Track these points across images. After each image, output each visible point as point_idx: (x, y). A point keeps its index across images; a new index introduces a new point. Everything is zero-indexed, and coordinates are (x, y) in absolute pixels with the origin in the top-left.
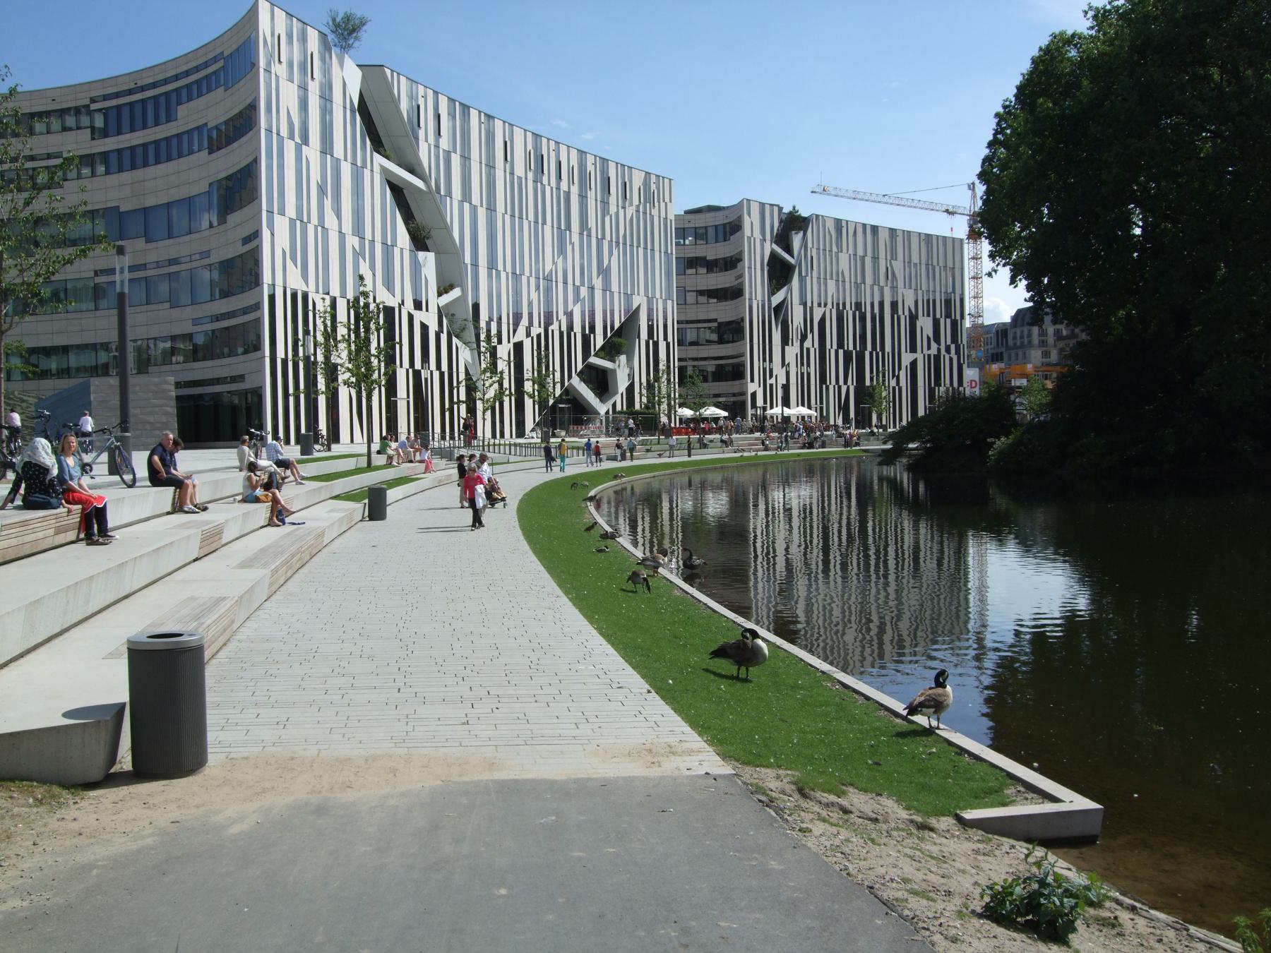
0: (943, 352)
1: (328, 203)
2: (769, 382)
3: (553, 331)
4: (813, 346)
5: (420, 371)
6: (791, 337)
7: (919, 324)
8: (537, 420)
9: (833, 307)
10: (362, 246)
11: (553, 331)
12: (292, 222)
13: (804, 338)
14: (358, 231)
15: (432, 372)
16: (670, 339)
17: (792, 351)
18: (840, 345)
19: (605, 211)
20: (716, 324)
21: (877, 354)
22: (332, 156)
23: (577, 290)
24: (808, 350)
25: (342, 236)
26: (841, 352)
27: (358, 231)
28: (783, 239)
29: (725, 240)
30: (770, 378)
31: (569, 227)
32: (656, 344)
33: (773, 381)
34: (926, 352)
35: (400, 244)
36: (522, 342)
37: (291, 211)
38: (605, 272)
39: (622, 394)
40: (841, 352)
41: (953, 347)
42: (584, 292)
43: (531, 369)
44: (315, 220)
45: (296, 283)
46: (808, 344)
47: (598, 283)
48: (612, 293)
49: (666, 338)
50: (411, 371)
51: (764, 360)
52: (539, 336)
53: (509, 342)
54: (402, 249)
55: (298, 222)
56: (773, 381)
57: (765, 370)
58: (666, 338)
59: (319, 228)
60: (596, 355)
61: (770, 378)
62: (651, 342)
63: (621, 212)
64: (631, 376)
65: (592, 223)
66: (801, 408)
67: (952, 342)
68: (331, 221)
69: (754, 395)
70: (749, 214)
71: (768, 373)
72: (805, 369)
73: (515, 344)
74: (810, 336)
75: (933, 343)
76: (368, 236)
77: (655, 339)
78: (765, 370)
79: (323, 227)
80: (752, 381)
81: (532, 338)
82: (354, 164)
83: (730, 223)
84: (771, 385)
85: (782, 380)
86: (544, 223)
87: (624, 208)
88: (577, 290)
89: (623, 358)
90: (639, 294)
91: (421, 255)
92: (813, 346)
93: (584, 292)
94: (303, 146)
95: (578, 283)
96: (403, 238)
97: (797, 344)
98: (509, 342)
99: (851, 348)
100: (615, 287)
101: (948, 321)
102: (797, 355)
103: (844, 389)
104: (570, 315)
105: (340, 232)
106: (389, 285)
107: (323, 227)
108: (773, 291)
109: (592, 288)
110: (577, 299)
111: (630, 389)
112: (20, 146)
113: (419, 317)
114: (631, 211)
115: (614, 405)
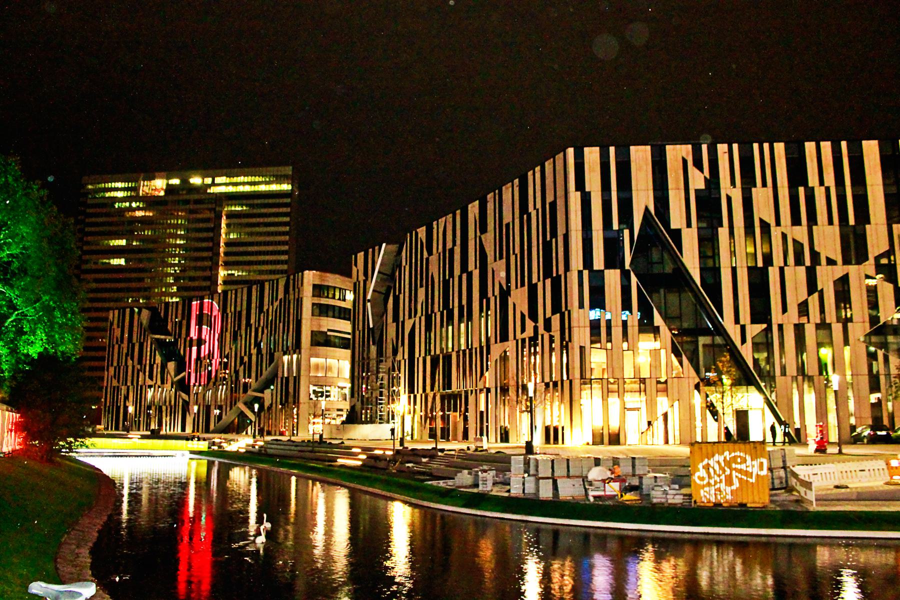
1: (129, 358)
9: (422, 315)
12: (115, 368)
13: (395, 352)
14: (140, 362)
23: (242, 358)
25: (133, 367)
27: (140, 362)
31: (240, 328)
34: (519, 336)
37: (115, 364)
41: (556, 320)
42: (246, 359)
44: (123, 364)
46: (399, 357)
47: (254, 351)
48: (262, 355)
63: (271, 307)
65: (252, 321)
68: (130, 362)
70: (356, 265)
74: (400, 349)
75: (528, 321)
76: (144, 362)
86: (226, 331)
87: (272, 304)
88: (242, 358)
90: (278, 351)
93: (246, 359)
95: (243, 354)
99: (438, 352)
101: (548, 282)
103: (431, 395)
106: (151, 378)
109: (250, 355)
110: (242, 362)
114: (276, 304)
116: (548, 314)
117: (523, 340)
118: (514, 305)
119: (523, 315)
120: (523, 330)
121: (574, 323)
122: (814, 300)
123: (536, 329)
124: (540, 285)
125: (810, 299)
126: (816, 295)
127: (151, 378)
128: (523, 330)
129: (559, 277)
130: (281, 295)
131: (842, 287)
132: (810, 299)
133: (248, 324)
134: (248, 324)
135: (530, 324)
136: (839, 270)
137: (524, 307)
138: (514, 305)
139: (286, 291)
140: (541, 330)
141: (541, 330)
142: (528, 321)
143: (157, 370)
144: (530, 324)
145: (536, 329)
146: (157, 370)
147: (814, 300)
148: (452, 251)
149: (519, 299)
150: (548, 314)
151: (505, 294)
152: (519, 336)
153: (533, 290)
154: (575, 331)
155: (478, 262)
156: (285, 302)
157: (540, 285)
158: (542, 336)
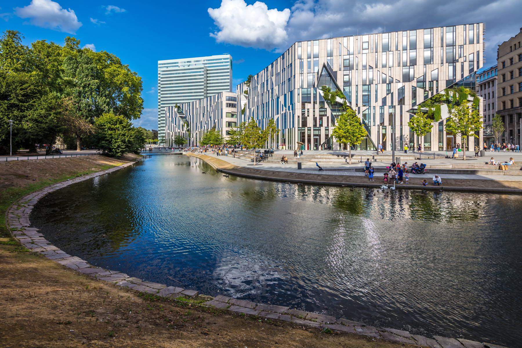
7: (280, 100)
19: (211, 106)
34: (282, 113)
38: (210, 117)
42: (207, 122)
45: (168, 131)
47: (209, 120)
65: (208, 110)
72: (491, 101)
75: (284, 107)
93: (207, 122)
100: (212, 120)
101: (289, 93)
104: (204, 127)
106: (179, 129)
112: (137, 124)
113: (183, 132)
114: (215, 103)
116: (289, 105)
119: (283, 105)
120: (283, 110)
121: (296, 108)
122: (389, 98)
123: (286, 109)
124: (287, 94)
125: (387, 96)
126: (390, 95)
127: (179, 129)
128: (283, 110)
129: (292, 91)
130: (216, 100)
131: (402, 91)
132: (387, 96)
133: (207, 111)
134: (207, 111)
135: (284, 108)
136: (400, 85)
137: (283, 103)
139: (218, 99)
140: (287, 111)
141: (287, 111)
142: (284, 107)
143: (181, 127)
144: (284, 108)
146: (181, 127)
147: (389, 98)
148: (264, 83)
149: (282, 99)
150: (289, 105)
151: (278, 98)
152: (282, 113)
153: (285, 95)
154: (296, 110)
156: (218, 103)
157: (287, 94)
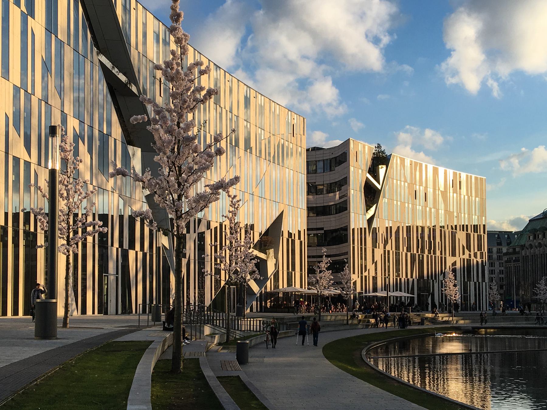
0: (472, 257)
2: (364, 274)
3: (225, 226)
4: (392, 249)
5: (186, 235)
6: (378, 242)
8: (213, 297)
10: (82, 129)
11: (225, 226)
15: (137, 252)
16: (302, 239)
17: (379, 252)
18: (409, 249)
20: (323, 232)
21: (431, 256)
22: (56, 37)
24: (389, 251)
26: (409, 254)
28: (373, 171)
29: (331, 171)
30: (365, 271)
32: (293, 242)
33: (366, 274)
35: (113, 135)
36: (204, 232)
39: (271, 279)
40: (409, 254)
43: (210, 254)
46: (388, 247)
49: (299, 238)
50: (120, 249)
51: (361, 259)
52: (216, 228)
53: (195, 232)
54: (115, 140)
55: (22, 91)
56: (366, 274)
57: (362, 265)
58: (299, 238)
59: (43, 103)
60: (255, 247)
61: (365, 271)
62: (290, 239)
64: (276, 265)
66: (398, 292)
67: (478, 250)
69: (355, 283)
71: (363, 268)
73: (198, 234)
74: (390, 241)
77: (293, 238)
78: (362, 265)
79: (47, 103)
80: (354, 273)
81: (211, 230)
82: (76, 50)
83: (336, 158)
84: (366, 277)
85: (372, 274)
89: (272, 251)
91: (130, 148)
92: (392, 249)
94: (29, 17)
96: (117, 132)
97: (382, 246)
98: (195, 232)
99: (415, 252)
102: (382, 255)
105: (62, 112)
107: (47, 103)
108: (368, 207)
111: (276, 275)
115: (266, 288)
116: (476, 251)
117: (464, 259)
118: (459, 239)
119: (463, 247)
120: (464, 254)
123: (470, 255)
128: (464, 254)
135: (467, 252)
137: (464, 242)
138: (459, 239)
141: (472, 257)
144: (467, 252)
145: (470, 255)
155: (437, 204)
158: (473, 260)
